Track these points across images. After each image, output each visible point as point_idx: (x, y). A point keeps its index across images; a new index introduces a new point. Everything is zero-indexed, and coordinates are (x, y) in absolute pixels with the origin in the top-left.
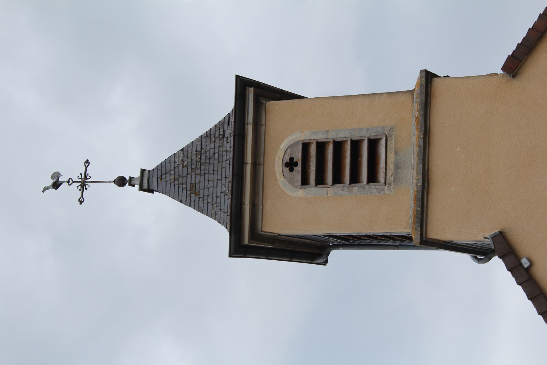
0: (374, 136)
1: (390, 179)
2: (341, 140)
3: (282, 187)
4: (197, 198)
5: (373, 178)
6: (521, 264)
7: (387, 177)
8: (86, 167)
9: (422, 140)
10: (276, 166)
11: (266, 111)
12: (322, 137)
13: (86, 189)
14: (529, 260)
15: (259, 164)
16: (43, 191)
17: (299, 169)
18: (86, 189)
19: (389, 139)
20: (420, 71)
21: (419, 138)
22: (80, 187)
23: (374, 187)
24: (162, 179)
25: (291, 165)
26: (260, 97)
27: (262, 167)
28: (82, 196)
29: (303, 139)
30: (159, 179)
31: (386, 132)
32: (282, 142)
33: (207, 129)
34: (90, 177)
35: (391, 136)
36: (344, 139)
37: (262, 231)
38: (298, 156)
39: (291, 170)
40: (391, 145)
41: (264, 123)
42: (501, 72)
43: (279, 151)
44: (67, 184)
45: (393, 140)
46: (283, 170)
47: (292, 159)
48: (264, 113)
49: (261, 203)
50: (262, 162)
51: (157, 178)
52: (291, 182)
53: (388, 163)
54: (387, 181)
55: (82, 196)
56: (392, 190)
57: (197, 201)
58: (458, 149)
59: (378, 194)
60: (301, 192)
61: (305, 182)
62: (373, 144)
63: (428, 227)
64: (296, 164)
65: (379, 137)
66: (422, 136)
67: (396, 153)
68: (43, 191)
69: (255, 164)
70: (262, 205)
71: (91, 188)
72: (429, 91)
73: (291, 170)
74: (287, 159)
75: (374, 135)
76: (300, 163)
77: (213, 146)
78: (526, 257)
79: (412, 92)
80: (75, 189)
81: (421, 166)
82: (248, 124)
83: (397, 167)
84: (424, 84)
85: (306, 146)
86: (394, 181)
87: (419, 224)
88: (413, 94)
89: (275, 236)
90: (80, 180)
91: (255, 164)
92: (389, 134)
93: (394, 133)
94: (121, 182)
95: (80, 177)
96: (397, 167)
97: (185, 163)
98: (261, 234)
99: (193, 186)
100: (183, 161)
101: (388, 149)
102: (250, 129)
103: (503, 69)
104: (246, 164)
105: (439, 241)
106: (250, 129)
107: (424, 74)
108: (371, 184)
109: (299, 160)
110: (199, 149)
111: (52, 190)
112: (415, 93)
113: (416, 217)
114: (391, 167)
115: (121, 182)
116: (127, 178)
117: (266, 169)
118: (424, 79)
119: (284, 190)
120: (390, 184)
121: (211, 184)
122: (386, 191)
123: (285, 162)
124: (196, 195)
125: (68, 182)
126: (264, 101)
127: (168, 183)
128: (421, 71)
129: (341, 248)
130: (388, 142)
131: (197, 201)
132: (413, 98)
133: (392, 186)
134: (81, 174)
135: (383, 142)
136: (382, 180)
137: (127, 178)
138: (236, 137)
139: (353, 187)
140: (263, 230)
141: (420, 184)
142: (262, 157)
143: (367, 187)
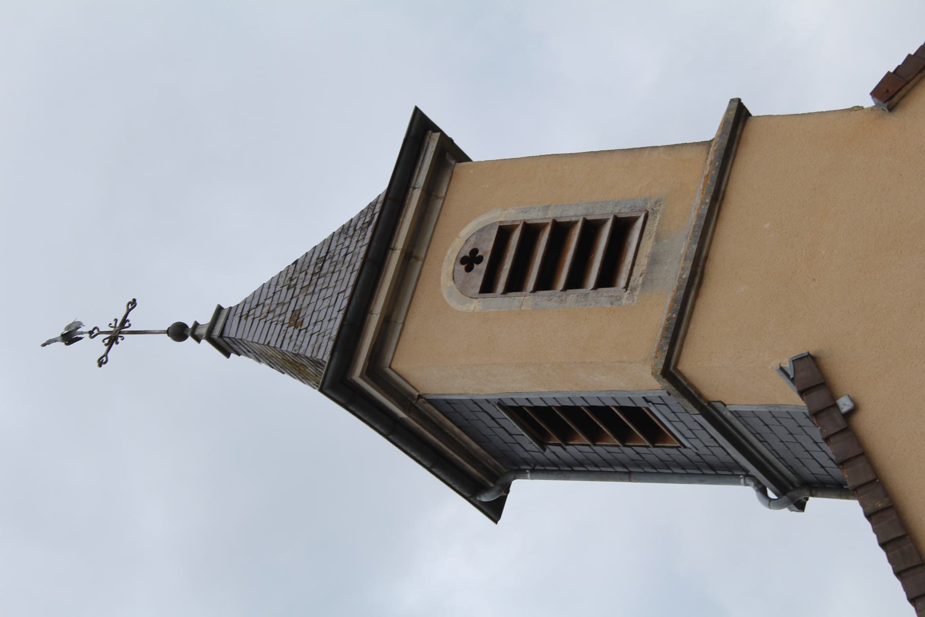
0: (625, 213)
1: (637, 279)
2: (568, 220)
3: (445, 296)
4: (296, 331)
5: (607, 279)
6: (835, 406)
7: (632, 278)
8: (129, 311)
9: (707, 207)
10: (445, 264)
11: (451, 177)
12: (535, 216)
13: (117, 343)
14: (852, 400)
15: (417, 258)
16: (44, 345)
17: (482, 267)
18: (117, 343)
19: (650, 217)
20: (729, 101)
21: (703, 203)
22: (107, 341)
23: (605, 294)
24: (248, 316)
25: (470, 261)
26: (447, 153)
27: (420, 263)
28: (106, 355)
29: (502, 219)
30: (243, 318)
31: (648, 207)
32: (465, 225)
33: (345, 221)
34: (130, 325)
35: (654, 212)
36: (574, 219)
37: (390, 367)
38: (486, 248)
39: (469, 269)
40: (652, 226)
41: (443, 194)
42: (869, 103)
43: (457, 239)
44: (88, 335)
45: (658, 219)
46: (456, 268)
47: (474, 251)
48: (447, 180)
49: (401, 321)
50: (422, 255)
51: (241, 317)
52: (463, 290)
53: (639, 256)
54: (631, 284)
55: (106, 355)
56: (636, 298)
57: (294, 337)
58: (767, 226)
59: (609, 306)
60: (478, 305)
61: (488, 287)
62: (622, 227)
63: (684, 350)
64: (480, 260)
65: (634, 215)
66: (708, 201)
67: (658, 239)
68: (44, 345)
69: (409, 256)
70: (403, 324)
71: (127, 342)
72: (738, 133)
73: (469, 269)
74: (466, 252)
75: (626, 210)
76: (486, 259)
77: (347, 243)
78: (849, 396)
79: (708, 144)
80: (98, 346)
81: (695, 247)
82: (414, 188)
83: (654, 261)
84: (732, 120)
85: (504, 233)
86: (643, 284)
87: (669, 340)
88: (710, 146)
89: (411, 395)
90: (112, 329)
91: (409, 256)
92: (652, 209)
93: (662, 207)
94: (179, 332)
95: (113, 325)
96: (654, 261)
97: (293, 283)
98: (386, 375)
99: (296, 314)
100: (291, 279)
101: (646, 233)
102: (415, 196)
103: (874, 94)
104: (394, 249)
105: (700, 395)
106: (415, 196)
107: (736, 104)
108: (601, 290)
109: (486, 253)
110: (323, 254)
111: (62, 345)
112: (713, 144)
113: (666, 329)
114: (643, 261)
115: (179, 332)
116: (190, 326)
117: (426, 267)
118: (733, 113)
119: (448, 300)
120: (633, 289)
121: (326, 303)
122: (624, 301)
123: (462, 255)
124: (296, 327)
125: (91, 332)
126: (453, 162)
127: (256, 321)
128: (732, 101)
129: (529, 475)
130: (648, 223)
131: (294, 337)
132: (708, 153)
133: (637, 293)
134: (116, 320)
135: (640, 221)
136: (622, 282)
137: (190, 326)
138: (388, 202)
139: (568, 295)
140: (393, 366)
141: (686, 275)
142: (424, 251)
143: (593, 294)
